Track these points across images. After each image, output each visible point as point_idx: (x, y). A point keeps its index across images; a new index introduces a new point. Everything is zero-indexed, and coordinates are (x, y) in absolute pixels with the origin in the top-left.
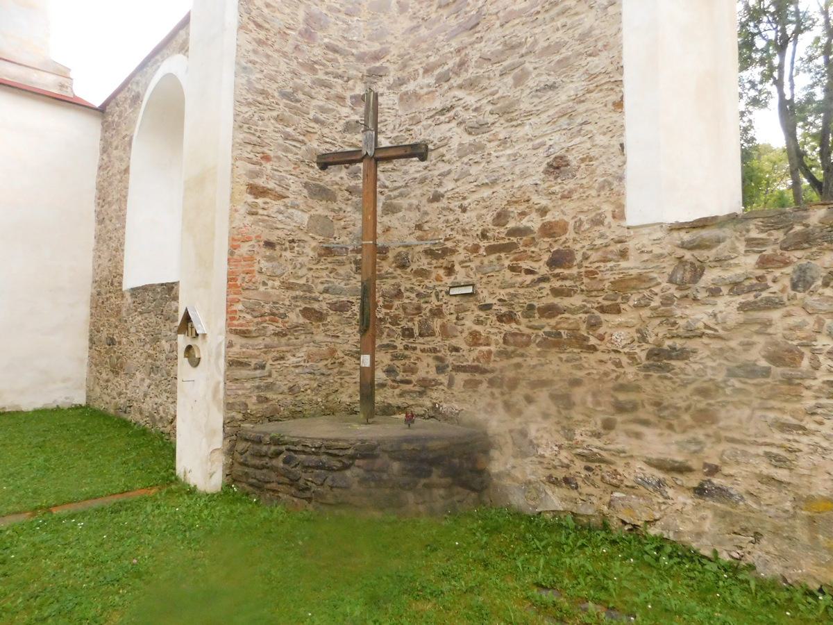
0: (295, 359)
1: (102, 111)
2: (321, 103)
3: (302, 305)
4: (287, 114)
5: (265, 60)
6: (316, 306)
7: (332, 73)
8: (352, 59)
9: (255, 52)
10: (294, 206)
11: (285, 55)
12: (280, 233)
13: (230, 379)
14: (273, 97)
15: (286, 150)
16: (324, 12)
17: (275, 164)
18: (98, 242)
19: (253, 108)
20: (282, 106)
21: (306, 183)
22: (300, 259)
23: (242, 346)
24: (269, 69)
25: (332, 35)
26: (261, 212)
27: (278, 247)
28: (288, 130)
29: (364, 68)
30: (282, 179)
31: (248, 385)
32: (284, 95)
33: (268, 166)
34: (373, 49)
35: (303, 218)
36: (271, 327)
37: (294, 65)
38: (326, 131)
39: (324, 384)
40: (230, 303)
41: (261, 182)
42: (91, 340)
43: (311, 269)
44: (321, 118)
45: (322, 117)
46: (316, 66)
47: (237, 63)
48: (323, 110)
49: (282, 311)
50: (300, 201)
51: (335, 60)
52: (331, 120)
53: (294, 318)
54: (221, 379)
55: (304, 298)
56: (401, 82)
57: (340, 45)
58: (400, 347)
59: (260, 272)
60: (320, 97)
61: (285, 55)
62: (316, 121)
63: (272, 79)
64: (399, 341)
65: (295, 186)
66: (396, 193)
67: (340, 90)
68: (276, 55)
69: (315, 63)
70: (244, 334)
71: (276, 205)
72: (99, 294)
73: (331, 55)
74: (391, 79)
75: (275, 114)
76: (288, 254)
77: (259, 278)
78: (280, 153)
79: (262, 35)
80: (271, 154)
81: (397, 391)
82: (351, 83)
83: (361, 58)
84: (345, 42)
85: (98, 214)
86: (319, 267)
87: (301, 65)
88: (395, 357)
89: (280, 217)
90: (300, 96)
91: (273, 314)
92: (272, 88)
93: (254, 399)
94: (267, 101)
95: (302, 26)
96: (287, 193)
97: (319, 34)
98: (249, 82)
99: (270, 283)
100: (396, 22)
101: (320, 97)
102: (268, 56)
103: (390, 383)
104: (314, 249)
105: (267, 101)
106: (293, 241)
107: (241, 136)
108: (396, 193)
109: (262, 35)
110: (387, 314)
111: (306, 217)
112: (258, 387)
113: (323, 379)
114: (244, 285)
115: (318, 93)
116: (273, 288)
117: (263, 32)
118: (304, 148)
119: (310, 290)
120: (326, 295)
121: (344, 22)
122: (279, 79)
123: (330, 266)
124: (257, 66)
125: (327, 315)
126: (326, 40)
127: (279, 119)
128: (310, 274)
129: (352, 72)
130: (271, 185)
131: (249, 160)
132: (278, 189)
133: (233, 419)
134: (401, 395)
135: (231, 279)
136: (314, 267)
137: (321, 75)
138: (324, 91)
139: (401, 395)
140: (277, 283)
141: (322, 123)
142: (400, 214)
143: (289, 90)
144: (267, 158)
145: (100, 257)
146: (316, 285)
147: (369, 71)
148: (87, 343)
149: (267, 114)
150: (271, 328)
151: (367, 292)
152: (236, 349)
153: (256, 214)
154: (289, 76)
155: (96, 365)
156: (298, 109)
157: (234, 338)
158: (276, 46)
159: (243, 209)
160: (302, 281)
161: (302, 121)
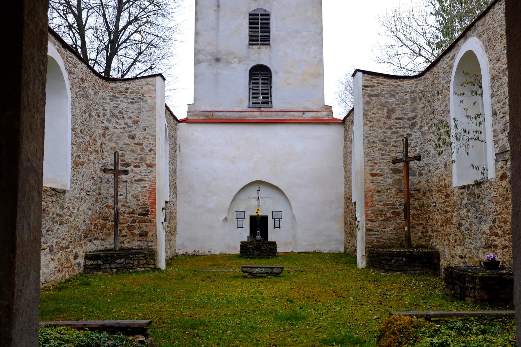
0: (390, 229)
1: (343, 122)
2: (395, 140)
3: (391, 210)
4: (382, 147)
5: (373, 132)
6: (397, 210)
7: (398, 128)
8: (405, 120)
9: (370, 130)
10: (386, 178)
11: (380, 127)
12: (382, 187)
13: (367, 235)
14: (377, 143)
15: (383, 159)
16: (394, 106)
17: (379, 165)
19: (370, 149)
20: (380, 145)
21: (391, 169)
22: (390, 195)
23: (371, 224)
24: (375, 134)
25: (398, 113)
26: (375, 181)
27: (382, 192)
28: (383, 152)
29: (410, 123)
30: (381, 169)
31: (373, 237)
32: (381, 141)
33: (377, 166)
34: (412, 115)
35: (391, 181)
36: (380, 218)
37: (384, 129)
38: (398, 149)
39: (401, 237)
40: (366, 211)
41: (374, 172)
42: (345, 223)
43: (394, 198)
44: (396, 145)
45: (396, 144)
46: (392, 127)
47: (364, 136)
48: (396, 142)
49: (384, 213)
50: (389, 175)
51: (400, 122)
52: (399, 144)
53: (388, 215)
54: (364, 234)
55: (392, 208)
56: (421, 127)
57: (401, 116)
58: (424, 224)
59: (376, 201)
60: (395, 137)
61: (380, 127)
62: (394, 146)
63: (376, 137)
64: (424, 222)
65: (387, 170)
66: (421, 169)
67: (402, 133)
68: (377, 129)
69: (392, 126)
70: (371, 221)
71: (380, 178)
72: (346, 203)
73: (398, 121)
74: (418, 126)
75: (378, 148)
76: (386, 194)
77: (375, 202)
78: (381, 161)
79: (371, 124)
80: (377, 162)
81: (424, 240)
82: (406, 129)
83: (408, 119)
84: (403, 115)
85: (345, 168)
86: (397, 197)
87: (386, 128)
88: (423, 228)
89: (382, 182)
90: (387, 139)
91: (381, 214)
92: (377, 140)
93: (375, 241)
94: (375, 145)
95: (386, 115)
96: (384, 174)
97: (393, 115)
98: (368, 141)
99: (379, 204)
100: (419, 105)
101: (395, 137)
102: (374, 130)
103: (422, 237)
104: (395, 191)
105: (375, 145)
106: (387, 189)
107: (367, 159)
108: (421, 169)
109: (371, 124)
110: (420, 212)
111: (392, 180)
112: (377, 237)
113: (401, 236)
114: (371, 205)
115: (394, 136)
116: (380, 205)
117: (372, 123)
118: (390, 157)
119: (395, 205)
120: (400, 207)
121: (402, 107)
122: (379, 136)
123: (401, 196)
124: (371, 135)
125: (401, 213)
126: (395, 116)
127: (379, 150)
128: (395, 199)
129: (406, 125)
130: (378, 172)
131: (370, 166)
132: (381, 173)
133: (369, 247)
134: (425, 241)
135: (366, 204)
136: (396, 197)
137: (394, 130)
138: (396, 135)
139: (425, 241)
140: (382, 204)
141: (396, 146)
142: (423, 176)
143: (382, 139)
144: (376, 164)
146: (397, 203)
147: (412, 124)
148: (344, 225)
149: (376, 149)
150: (380, 218)
151: (407, 206)
152: (369, 225)
153: (374, 182)
154: (382, 134)
155: (347, 234)
156: (386, 144)
157: (367, 222)
158: (377, 126)
159: (369, 182)
160: (391, 202)
161: (388, 148)
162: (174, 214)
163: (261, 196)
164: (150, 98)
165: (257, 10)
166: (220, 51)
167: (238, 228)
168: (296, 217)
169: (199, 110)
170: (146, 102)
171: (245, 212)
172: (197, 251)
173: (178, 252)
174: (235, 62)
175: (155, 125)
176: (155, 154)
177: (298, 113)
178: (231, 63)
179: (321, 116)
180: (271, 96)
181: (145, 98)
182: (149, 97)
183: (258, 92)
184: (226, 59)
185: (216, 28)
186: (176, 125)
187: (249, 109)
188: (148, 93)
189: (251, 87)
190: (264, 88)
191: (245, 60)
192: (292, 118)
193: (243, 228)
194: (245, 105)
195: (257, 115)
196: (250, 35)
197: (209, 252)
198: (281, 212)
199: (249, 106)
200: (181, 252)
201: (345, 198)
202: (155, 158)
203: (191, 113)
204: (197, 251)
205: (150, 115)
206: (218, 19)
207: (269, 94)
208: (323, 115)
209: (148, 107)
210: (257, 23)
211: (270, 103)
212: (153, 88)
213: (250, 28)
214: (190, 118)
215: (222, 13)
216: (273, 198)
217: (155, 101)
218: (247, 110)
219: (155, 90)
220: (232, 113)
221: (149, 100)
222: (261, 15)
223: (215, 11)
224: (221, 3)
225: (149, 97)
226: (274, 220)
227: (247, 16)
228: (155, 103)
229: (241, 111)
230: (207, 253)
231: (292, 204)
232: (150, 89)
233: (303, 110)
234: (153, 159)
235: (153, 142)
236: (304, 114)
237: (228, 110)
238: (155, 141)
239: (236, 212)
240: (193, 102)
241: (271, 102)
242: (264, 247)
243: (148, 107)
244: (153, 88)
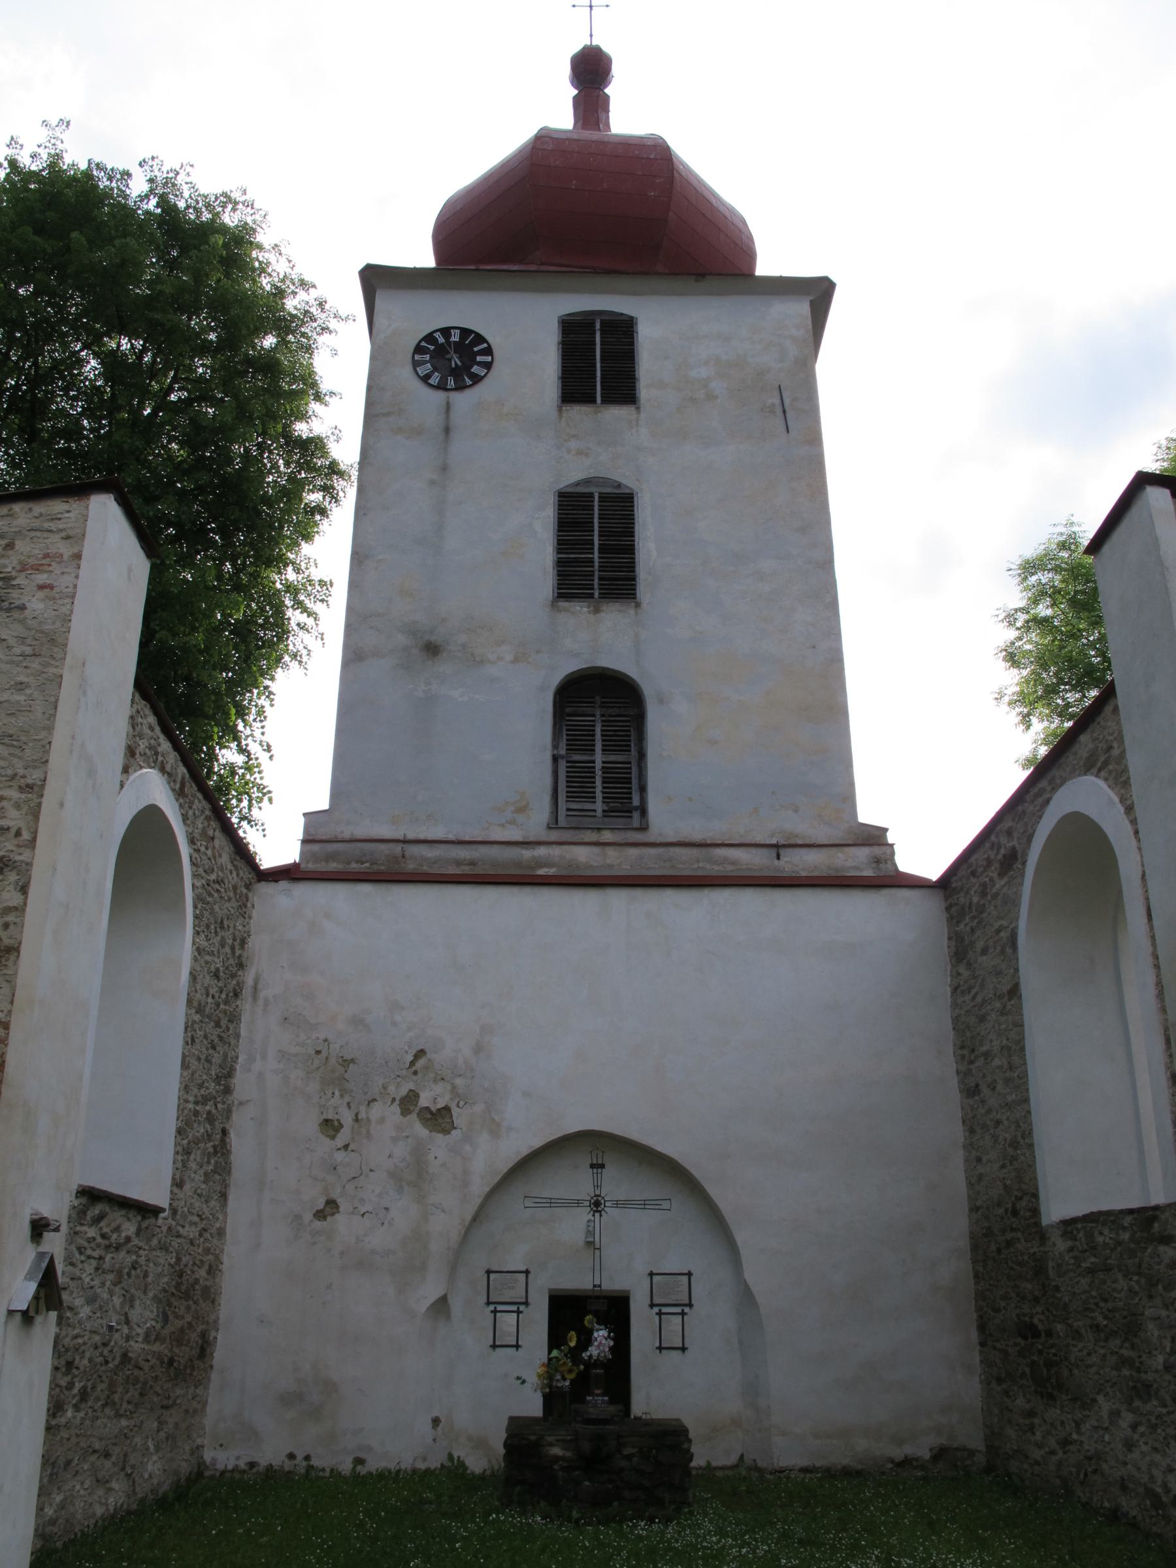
18: (972, 1131)
42: (982, 1328)
85: (964, 1075)
145: (979, 1160)
148: (974, 1335)
155: (999, 1380)
162: (202, 1273)
163: (584, 1215)
164: (41, 594)
165: (587, 481)
166: (444, 620)
167: (494, 1346)
168: (760, 1299)
169: (347, 835)
170: (16, 614)
171: (527, 1272)
172: (300, 1458)
173: (214, 1461)
174: (500, 658)
175: (50, 729)
176: (24, 889)
177: (753, 850)
178: (481, 662)
179: (850, 863)
180: (643, 789)
181: (15, 594)
182: (41, 587)
183: (592, 770)
186: (248, 886)
187: (554, 836)
188: (38, 568)
189: (563, 752)
190: (612, 758)
191: (538, 652)
192: (729, 870)
193: (517, 1346)
194: (537, 820)
195: (583, 856)
196: (560, 563)
197: (359, 1461)
198: (689, 1274)
199: (554, 824)
200: (223, 1458)
201: (974, 1209)
202: (20, 910)
203: (316, 847)
204: (300, 1458)
205: (31, 680)
207: (635, 781)
208: (856, 861)
209: (22, 640)
210: (588, 526)
211: (636, 815)
212: (66, 550)
214: (311, 866)
216: (666, 1205)
217: (65, 610)
218: (544, 838)
219: (78, 556)
220: (484, 850)
221: (36, 604)
222: (603, 498)
223: (432, 483)
225: (41, 587)
226: (660, 1314)
228: (67, 619)
229: (519, 838)
230: (346, 1467)
231: (740, 1237)
232: (52, 550)
233: (774, 841)
234: (10, 918)
235: (22, 824)
236: (778, 857)
237: (467, 838)
238: (36, 813)
239: (489, 1272)
240: (326, 806)
241: (643, 811)
242: (629, 1458)
243: (22, 640)
244: (66, 550)
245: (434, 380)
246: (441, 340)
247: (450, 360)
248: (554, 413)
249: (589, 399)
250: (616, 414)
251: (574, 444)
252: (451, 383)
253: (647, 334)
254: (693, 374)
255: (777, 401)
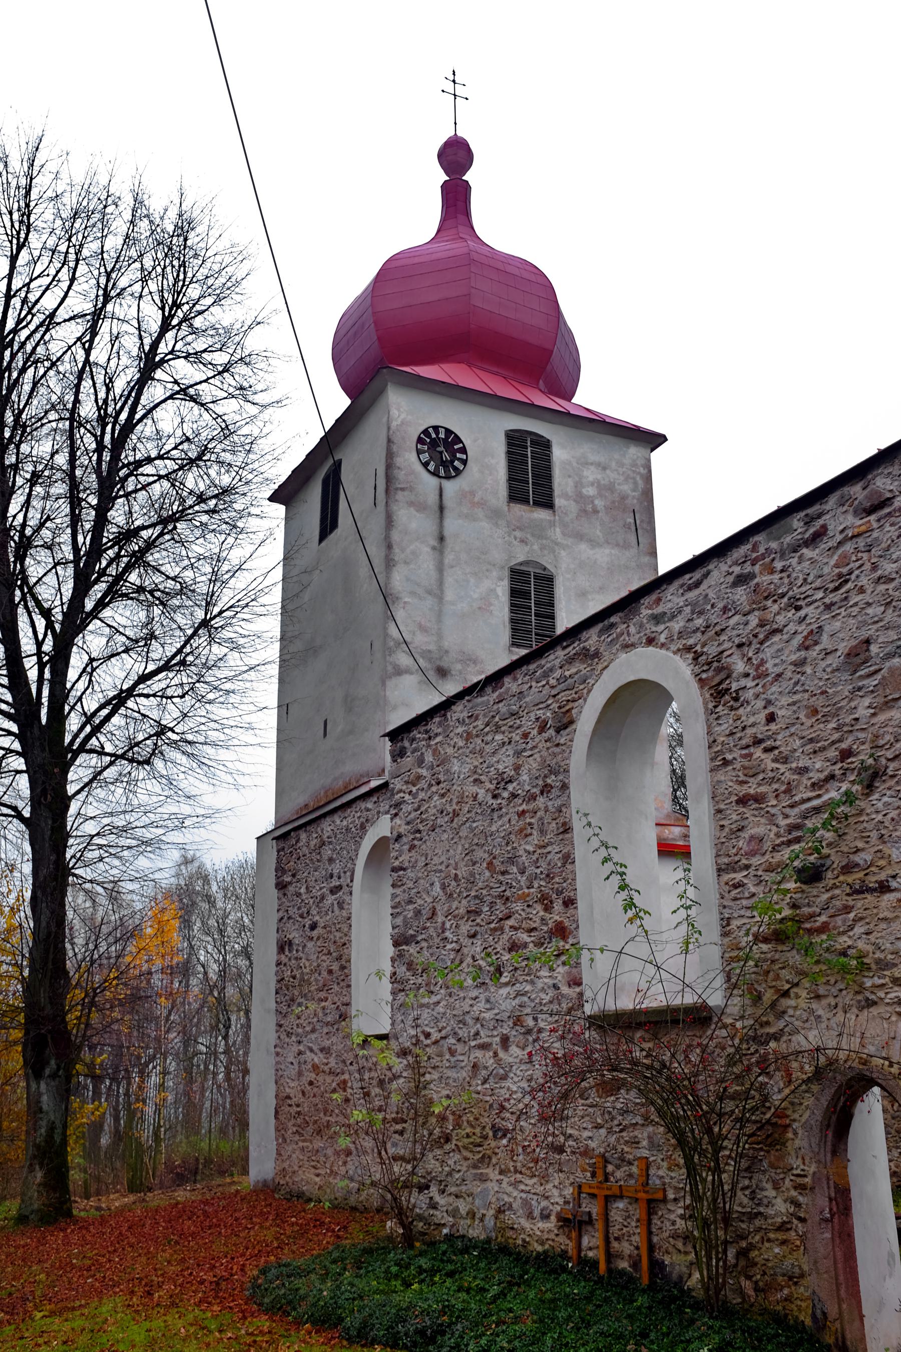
165: (526, 563)
166: (447, 652)
179: (671, 836)
184: (460, 672)
185: (438, 592)
196: (512, 621)
206: (440, 569)
210: (526, 595)
213: (512, 605)
215: (449, 558)
224: (447, 533)
227: (506, 573)
245: (432, 467)
246: (434, 436)
247: (441, 453)
248: (506, 508)
249: (525, 501)
250: (542, 514)
251: (518, 534)
252: (442, 473)
253: (559, 454)
254: (584, 491)
255: (632, 521)
